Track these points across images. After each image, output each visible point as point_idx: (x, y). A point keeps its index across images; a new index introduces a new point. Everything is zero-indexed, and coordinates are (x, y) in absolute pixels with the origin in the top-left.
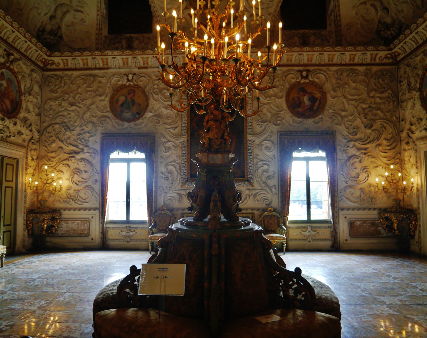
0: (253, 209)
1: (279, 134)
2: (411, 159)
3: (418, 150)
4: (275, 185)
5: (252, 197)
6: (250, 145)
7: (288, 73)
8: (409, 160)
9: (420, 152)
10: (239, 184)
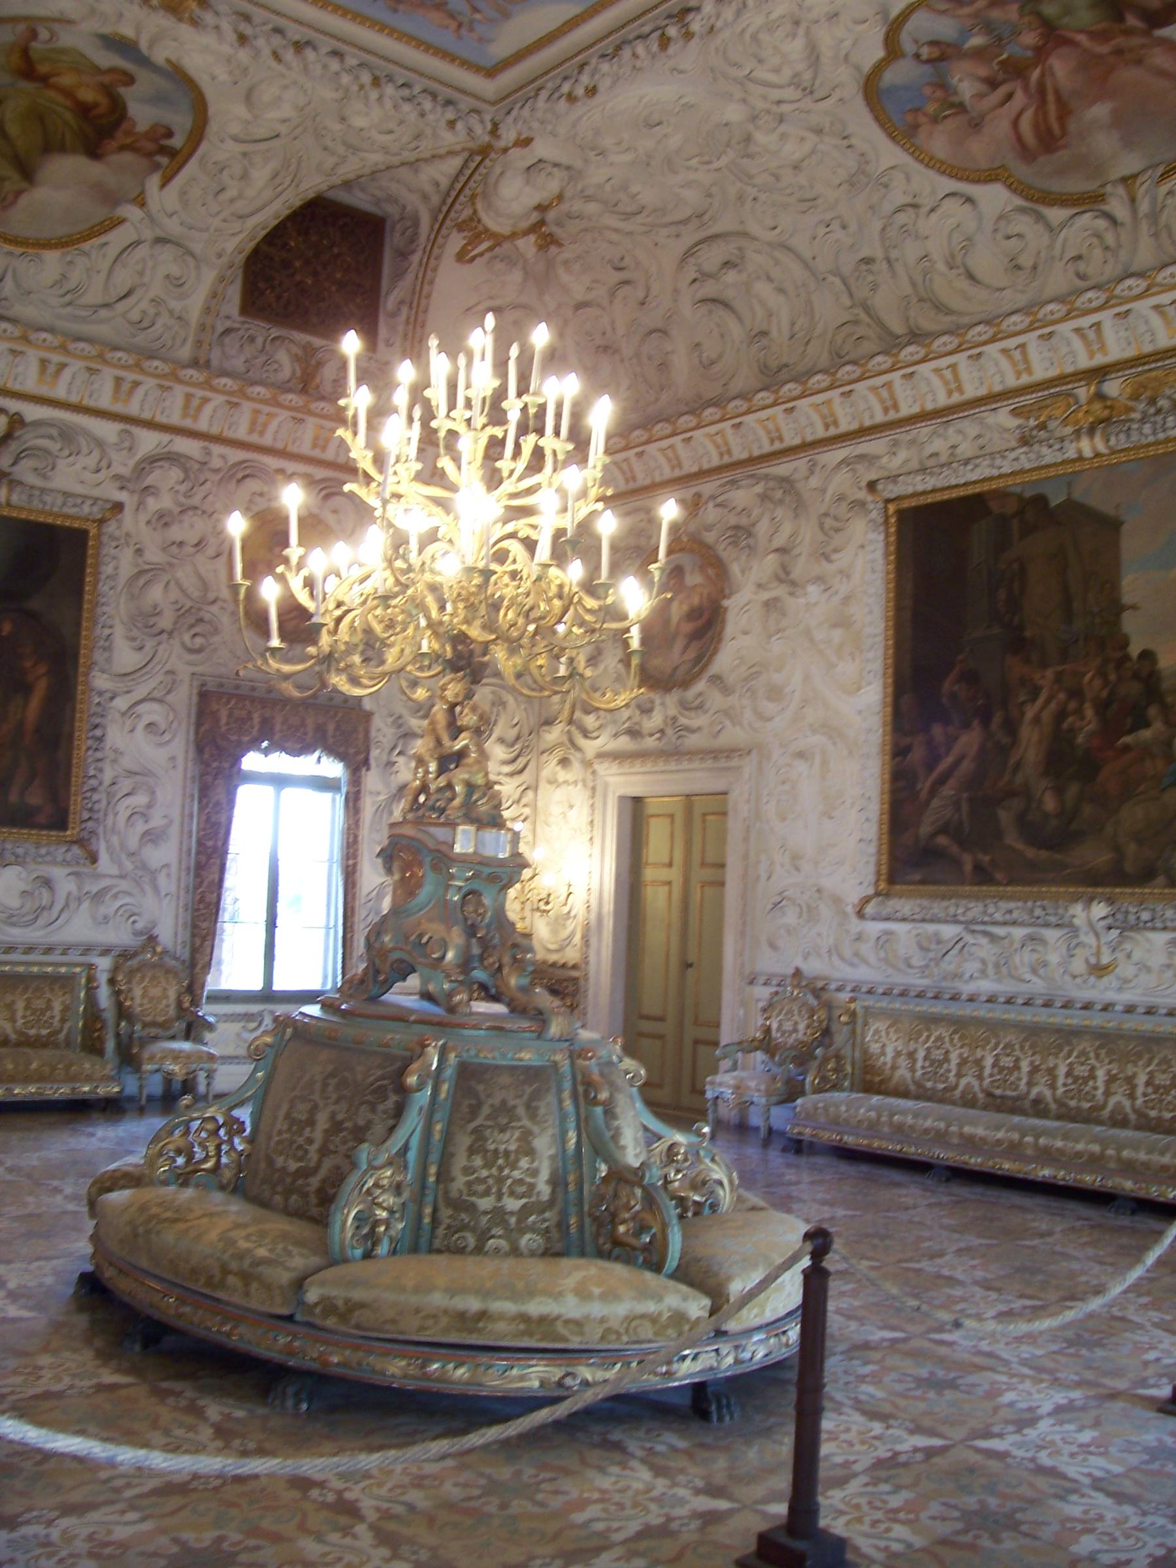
0: (87, 949)
1: (196, 683)
2: (572, 814)
3: (599, 790)
4: (167, 866)
5: (86, 905)
6: (99, 710)
7: (248, 472)
8: (564, 814)
9: (605, 796)
10: (48, 853)
